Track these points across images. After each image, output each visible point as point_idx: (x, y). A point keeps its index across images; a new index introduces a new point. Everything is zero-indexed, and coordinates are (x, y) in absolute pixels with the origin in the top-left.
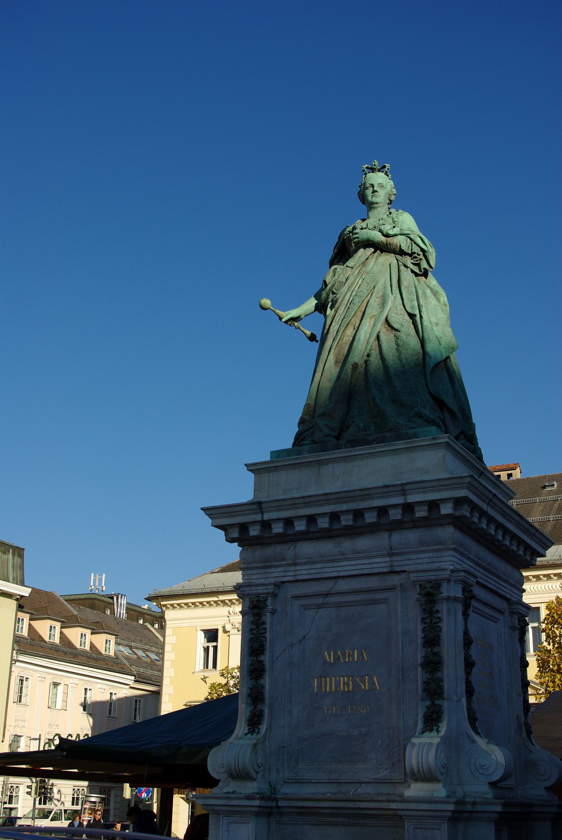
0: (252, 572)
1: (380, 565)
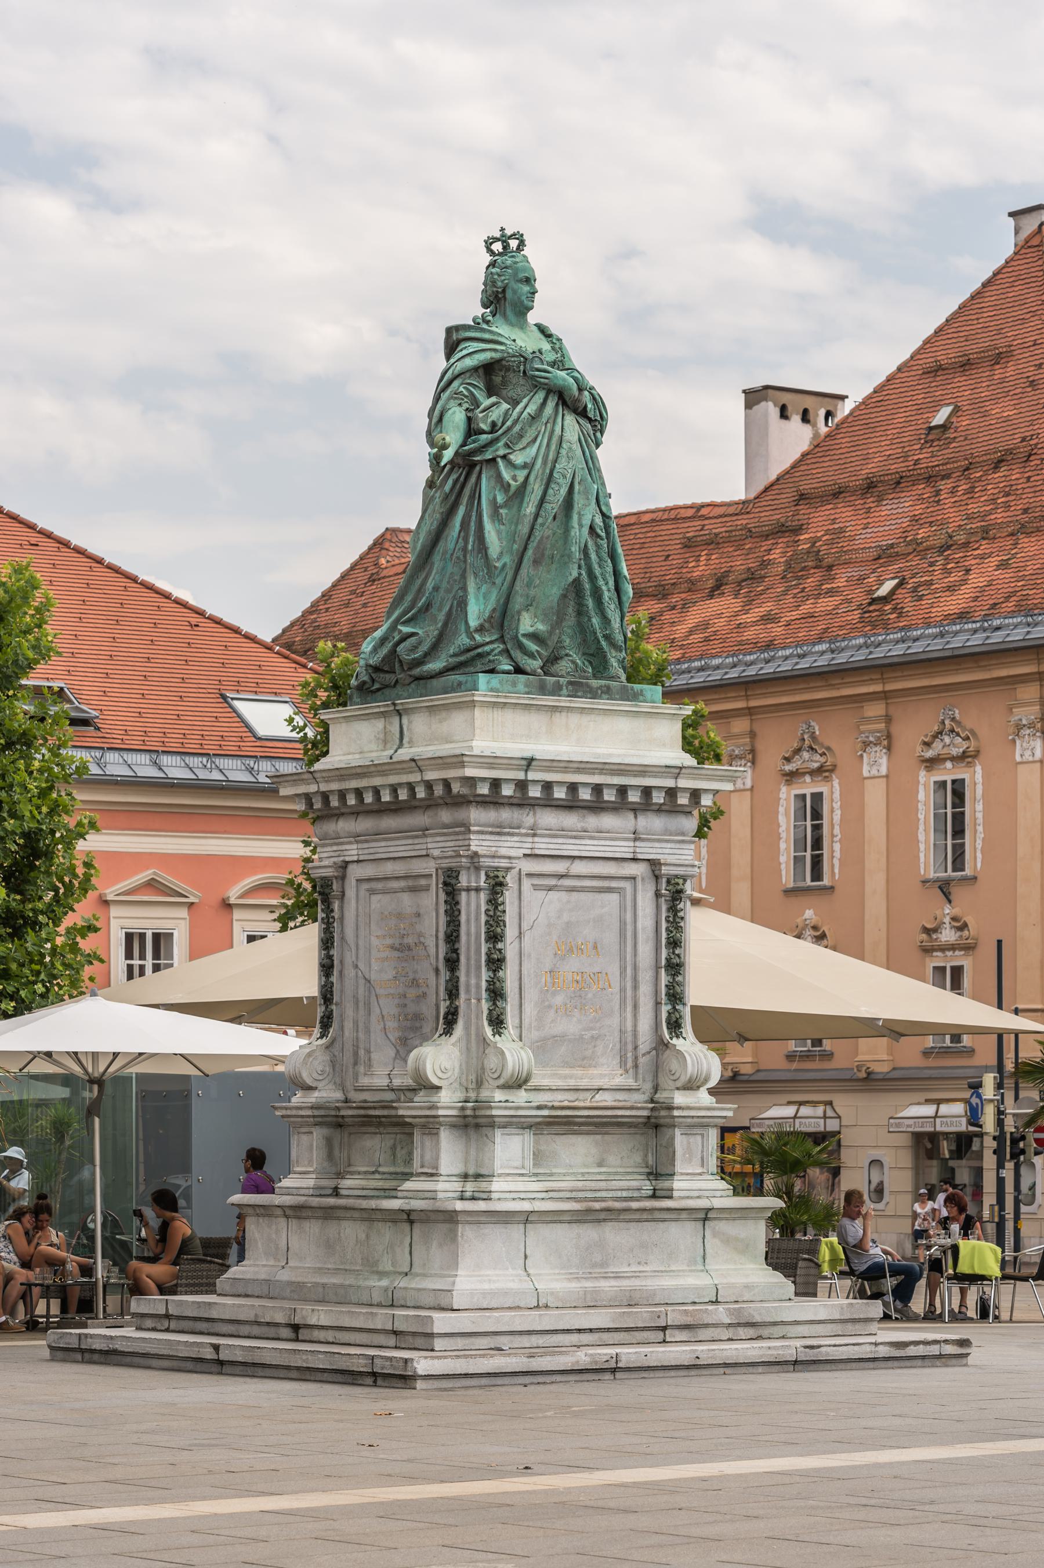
0: (483, 837)
1: (623, 849)
